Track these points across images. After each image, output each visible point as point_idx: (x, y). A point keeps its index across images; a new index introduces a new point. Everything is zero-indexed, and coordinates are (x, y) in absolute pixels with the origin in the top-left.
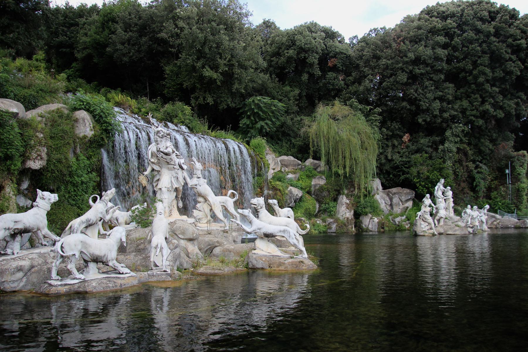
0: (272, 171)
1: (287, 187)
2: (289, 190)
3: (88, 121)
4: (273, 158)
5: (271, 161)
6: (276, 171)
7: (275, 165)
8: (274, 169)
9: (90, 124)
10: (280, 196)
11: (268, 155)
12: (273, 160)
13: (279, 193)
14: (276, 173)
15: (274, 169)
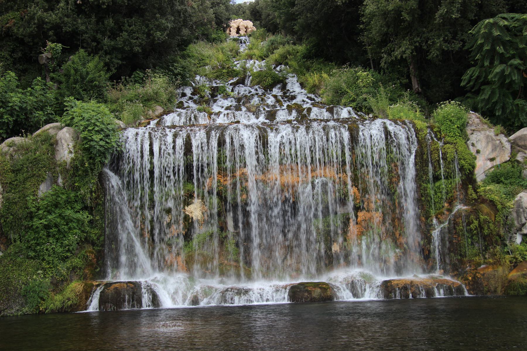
0: (489, 164)
1: (512, 195)
2: (516, 199)
3: (66, 141)
4: (488, 137)
5: (484, 144)
6: (498, 162)
7: (494, 149)
8: (492, 160)
9: (68, 145)
10: (487, 214)
11: (475, 133)
12: (488, 143)
13: (485, 208)
14: (497, 166)
15: (492, 160)
